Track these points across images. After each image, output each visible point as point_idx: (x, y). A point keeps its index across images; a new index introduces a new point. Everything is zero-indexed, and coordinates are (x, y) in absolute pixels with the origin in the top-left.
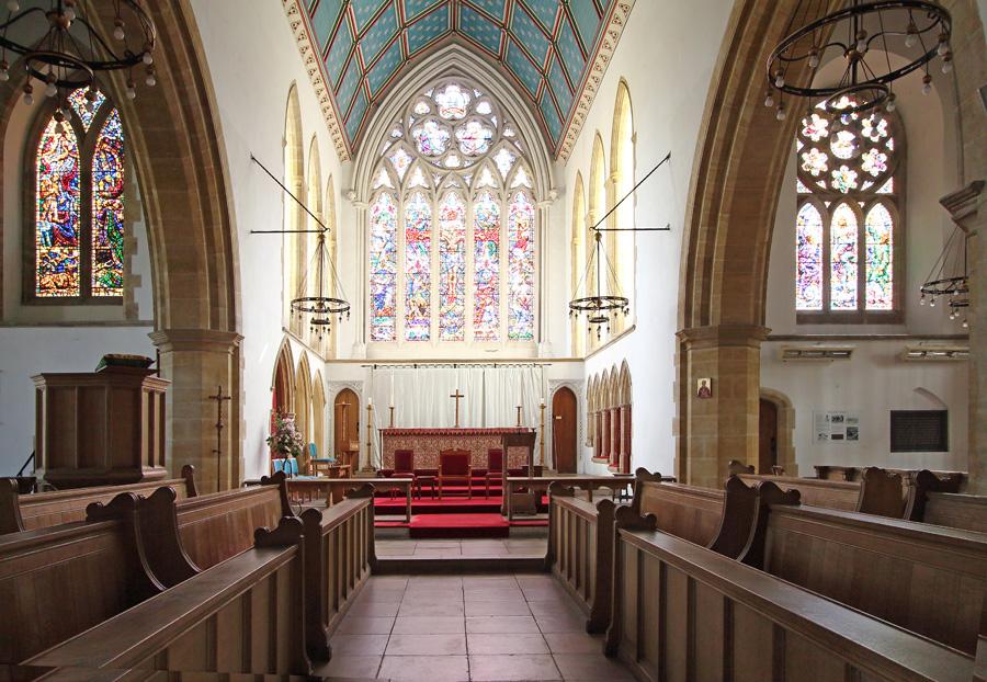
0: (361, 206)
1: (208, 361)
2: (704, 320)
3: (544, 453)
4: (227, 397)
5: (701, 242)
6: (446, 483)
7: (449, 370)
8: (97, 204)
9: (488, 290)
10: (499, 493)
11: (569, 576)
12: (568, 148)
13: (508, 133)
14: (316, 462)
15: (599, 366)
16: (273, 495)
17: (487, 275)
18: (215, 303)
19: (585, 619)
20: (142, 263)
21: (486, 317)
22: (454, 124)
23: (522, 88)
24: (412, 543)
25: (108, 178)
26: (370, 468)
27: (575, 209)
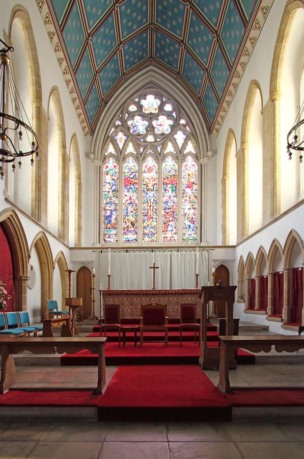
21: (170, 228)
22: (150, 117)
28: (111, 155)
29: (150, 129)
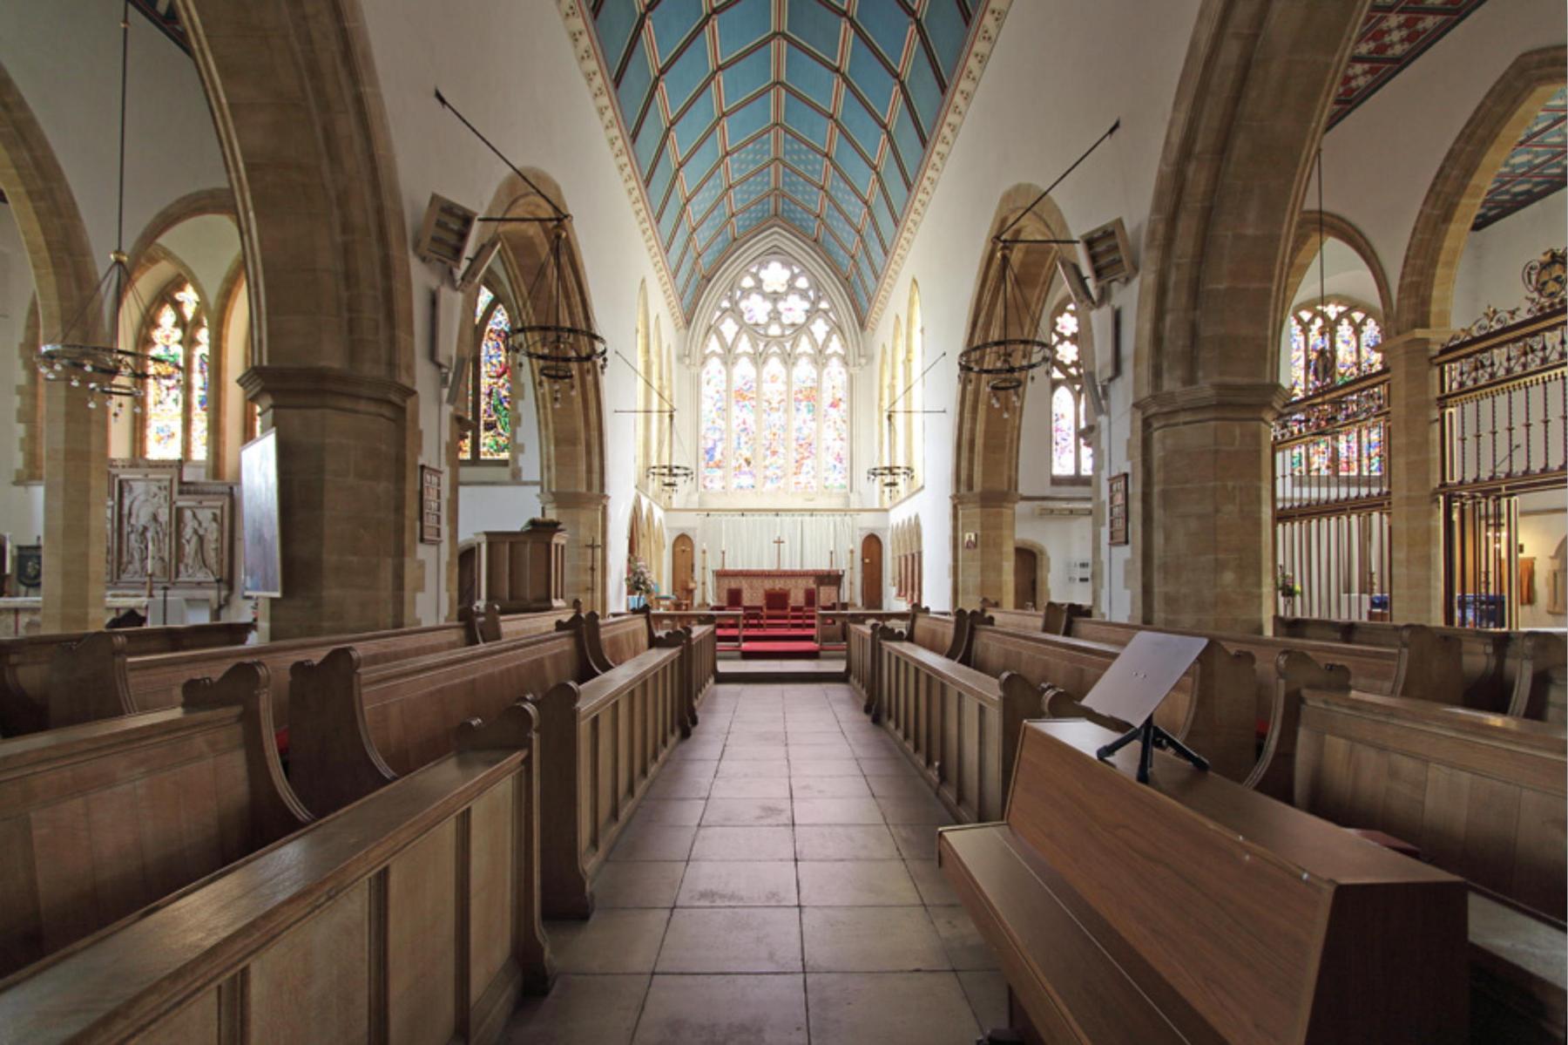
0: (694, 370)
1: (584, 516)
2: (970, 487)
3: (852, 592)
4: (598, 546)
5: (967, 426)
6: (769, 617)
7: (771, 517)
8: (485, 383)
9: (807, 447)
10: (812, 626)
11: (917, 748)
12: (921, 210)
13: (824, 305)
14: (659, 599)
15: (899, 516)
16: (640, 623)
17: (806, 432)
18: (589, 471)
19: (863, 703)
20: (529, 434)
21: (804, 469)
22: (775, 297)
23: (835, 268)
24: (744, 663)
25: (494, 361)
26: (704, 604)
27: (881, 380)
28: (713, 353)
29: (775, 316)
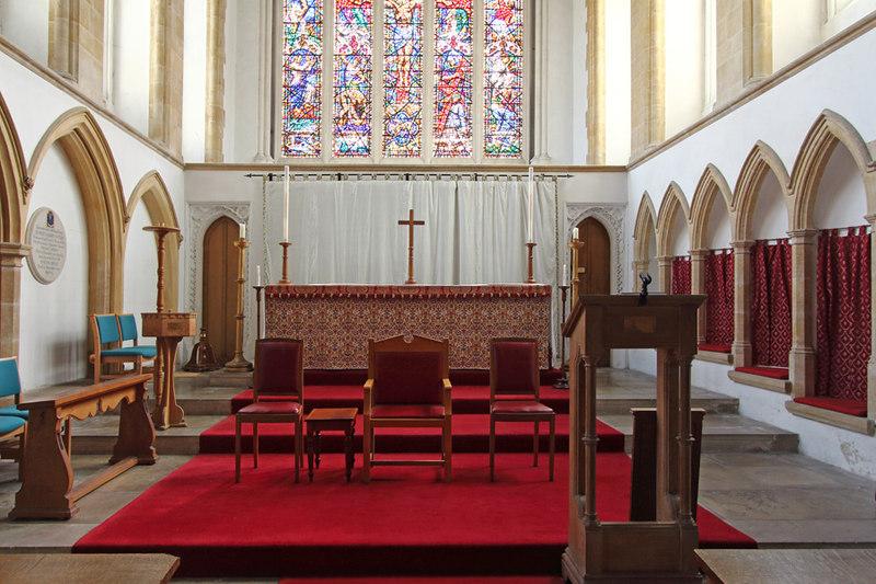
7: (395, 182)
17: (454, 59)
